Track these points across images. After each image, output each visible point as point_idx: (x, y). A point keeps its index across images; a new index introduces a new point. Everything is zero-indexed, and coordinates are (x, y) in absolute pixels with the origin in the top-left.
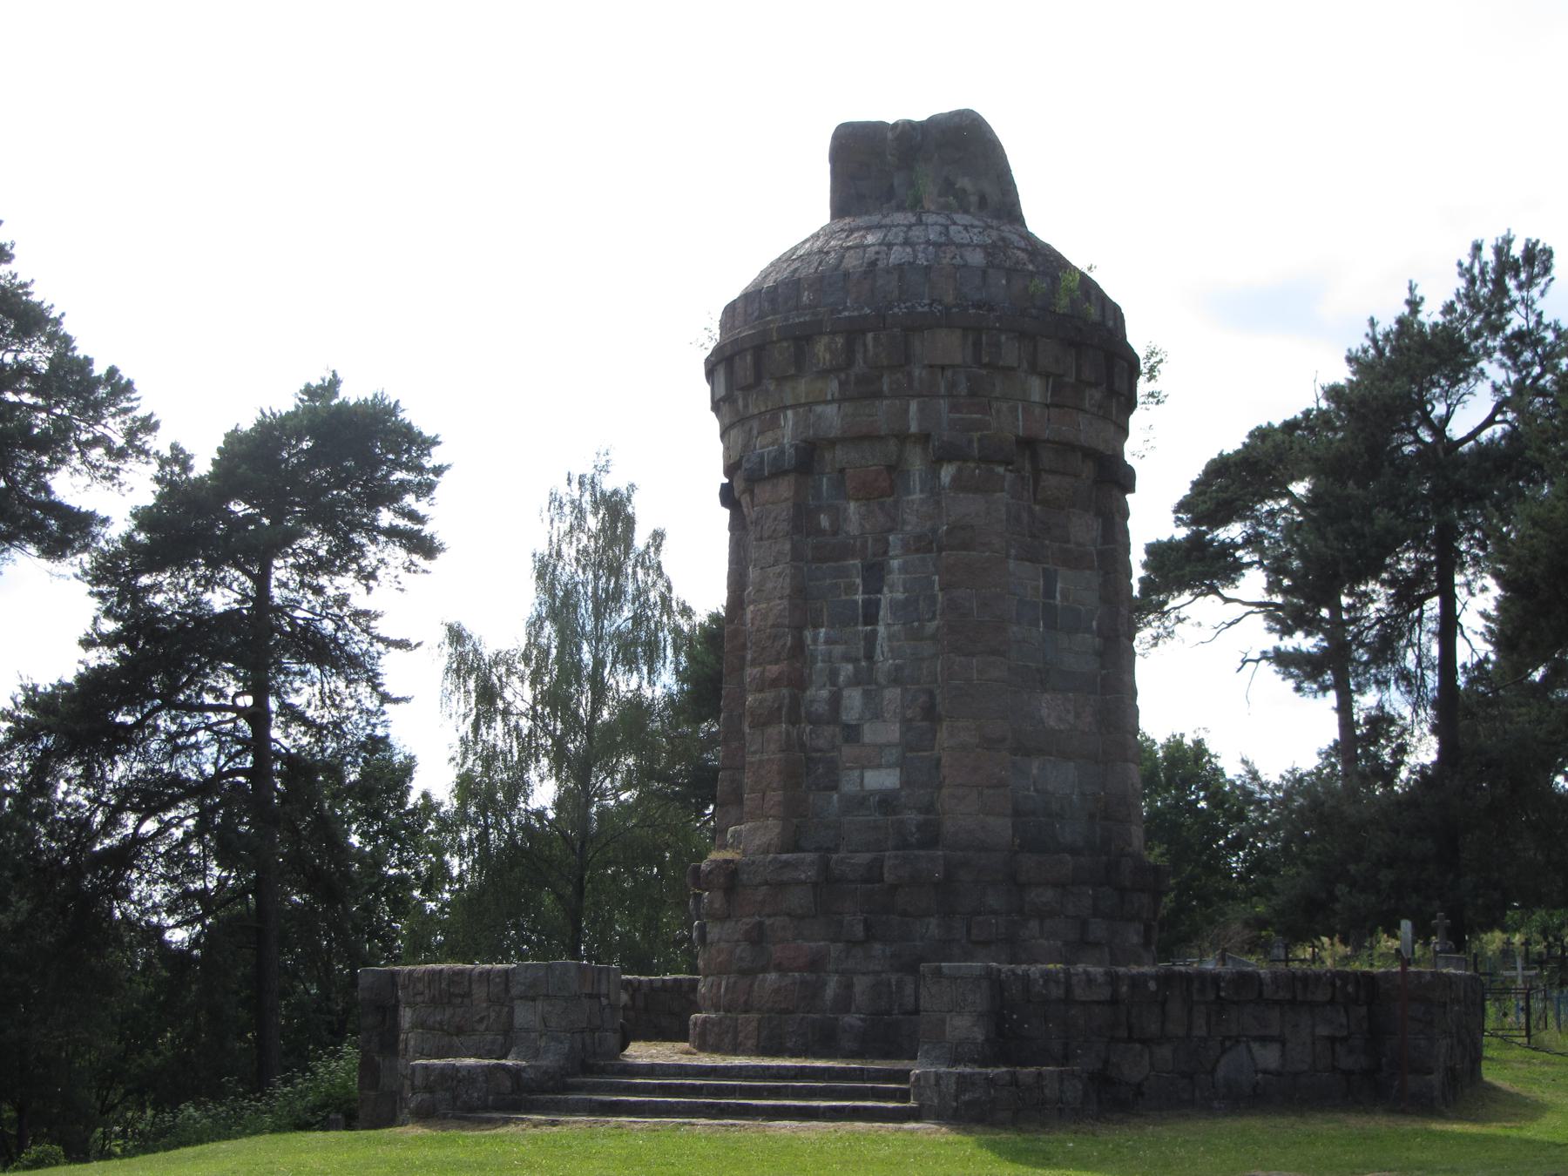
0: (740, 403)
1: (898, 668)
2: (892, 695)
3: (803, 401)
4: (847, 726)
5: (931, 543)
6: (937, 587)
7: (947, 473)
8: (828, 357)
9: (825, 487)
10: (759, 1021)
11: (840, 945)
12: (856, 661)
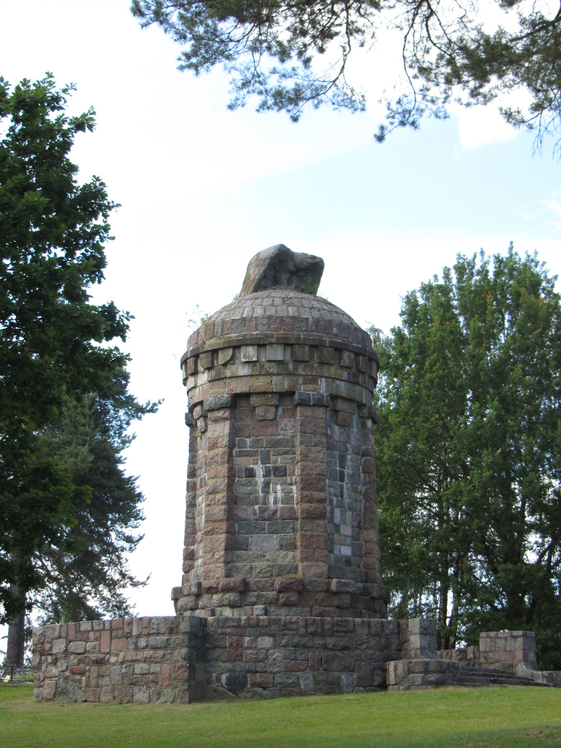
2: (349, 514)
3: (333, 376)
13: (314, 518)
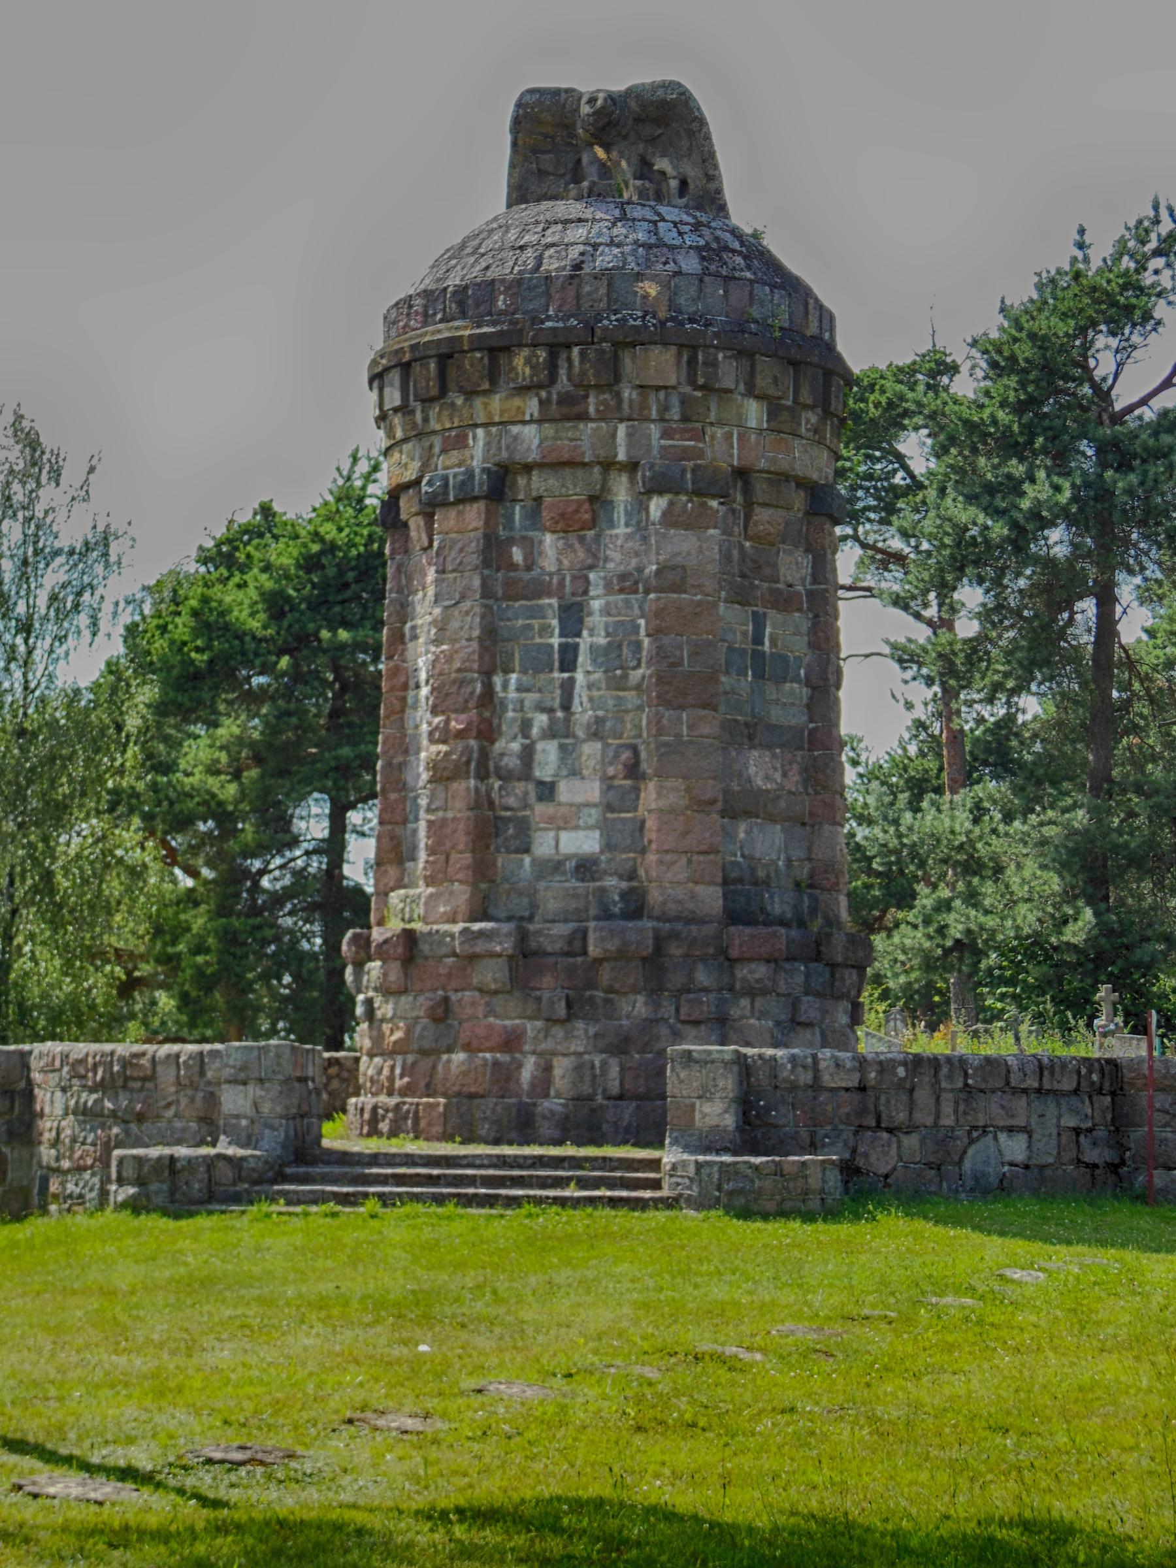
0: (419, 416)
1: (599, 721)
2: (591, 751)
3: (497, 419)
4: (540, 783)
5: (636, 583)
6: (642, 632)
7: (657, 506)
8: (528, 371)
9: (517, 517)
10: (446, 1106)
11: (539, 1024)
12: (550, 711)
13: (448, 779)
